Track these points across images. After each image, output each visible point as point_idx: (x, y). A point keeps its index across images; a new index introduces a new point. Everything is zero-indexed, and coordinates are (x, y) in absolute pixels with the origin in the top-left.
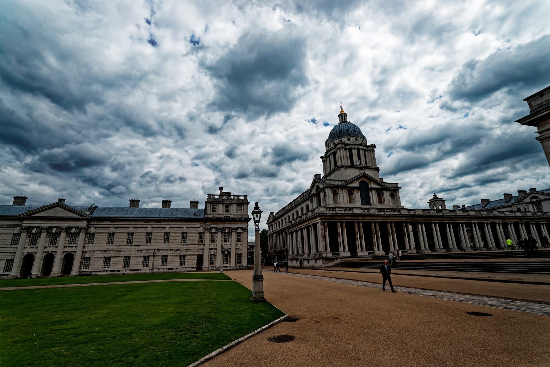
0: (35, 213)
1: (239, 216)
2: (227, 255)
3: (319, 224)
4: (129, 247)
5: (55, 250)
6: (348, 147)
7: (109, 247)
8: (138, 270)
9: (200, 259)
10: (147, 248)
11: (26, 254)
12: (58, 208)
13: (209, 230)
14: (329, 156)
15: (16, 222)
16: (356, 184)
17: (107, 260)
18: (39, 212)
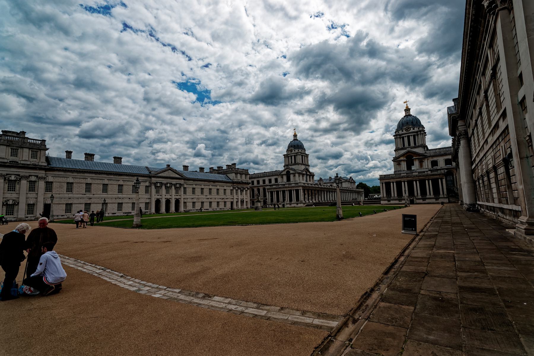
0: (159, 173)
1: (246, 181)
2: (242, 202)
3: (301, 190)
4: (202, 196)
5: (170, 197)
6: (302, 154)
7: (194, 196)
8: (208, 209)
9: (232, 203)
10: (210, 197)
11: (156, 199)
12: (170, 171)
13: (235, 188)
14: (291, 156)
15: (146, 178)
16: (304, 173)
17: (194, 203)
18: (161, 173)
